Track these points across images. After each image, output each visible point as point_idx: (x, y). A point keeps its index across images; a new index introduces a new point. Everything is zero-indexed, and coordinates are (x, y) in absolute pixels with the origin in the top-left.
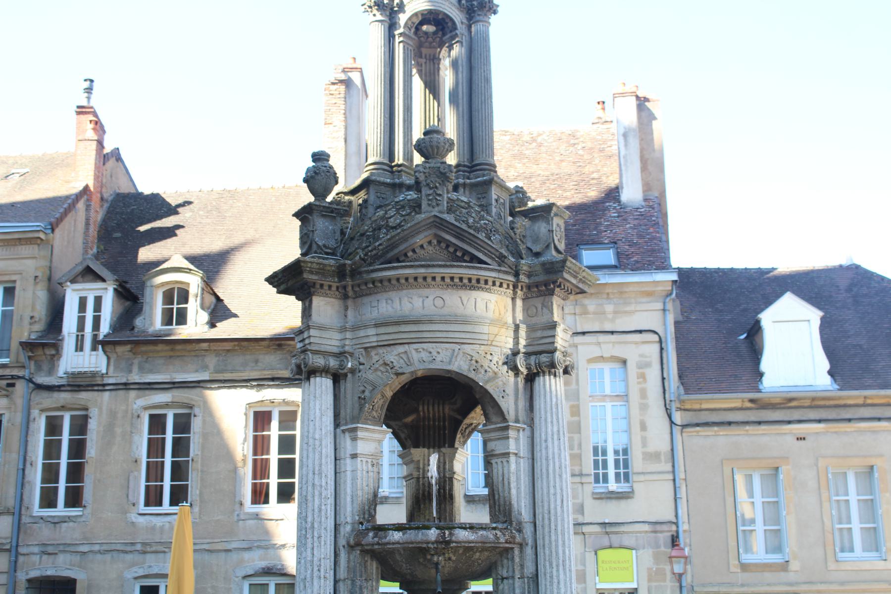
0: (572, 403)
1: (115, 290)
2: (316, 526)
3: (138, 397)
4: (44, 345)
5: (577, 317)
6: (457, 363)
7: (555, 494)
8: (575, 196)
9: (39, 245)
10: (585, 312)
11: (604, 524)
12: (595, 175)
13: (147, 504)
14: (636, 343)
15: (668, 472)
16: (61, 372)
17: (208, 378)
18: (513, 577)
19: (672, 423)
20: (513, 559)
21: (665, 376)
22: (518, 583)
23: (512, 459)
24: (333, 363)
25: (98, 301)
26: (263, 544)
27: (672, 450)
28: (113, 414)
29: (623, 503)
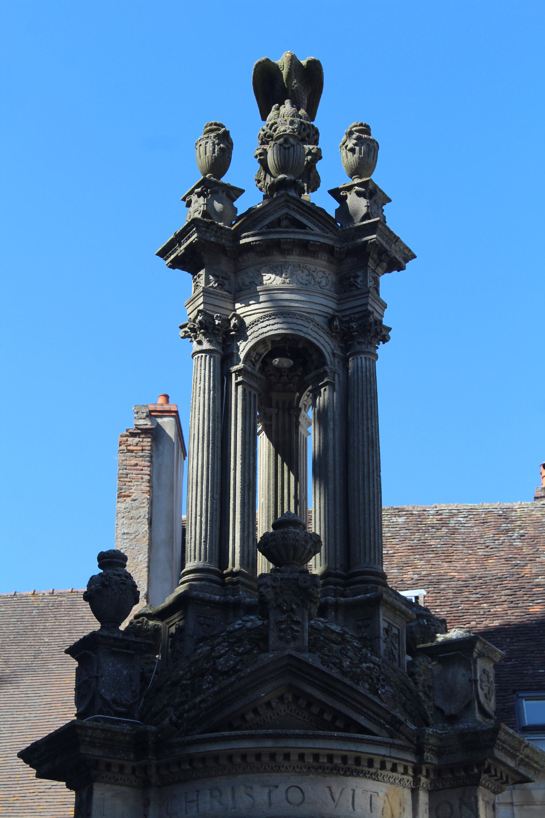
5: (516, 809)
8: (509, 612)
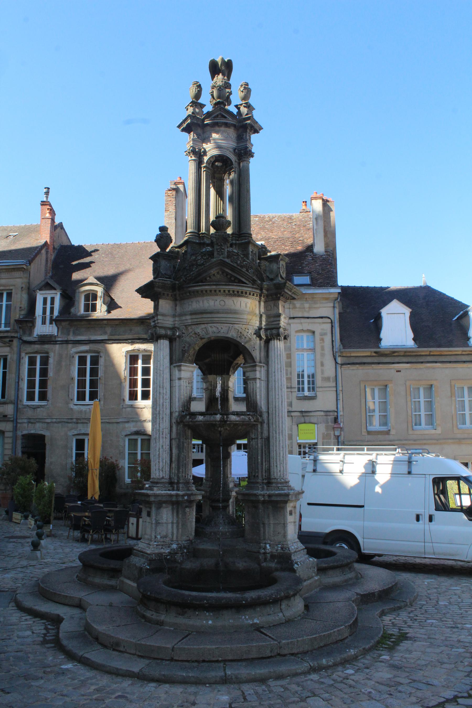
0: (287, 352)
1: (61, 294)
2: (161, 412)
3: (73, 347)
4: (26, 322)
6: (231, 334)
7: (278, 398)
9: (23, 271)
10: (295, 307)
11: (301, 412)
12: (301, 239)
13: (78, 400)
14: (320, 323)
15: (334, 387)
16: (35, 335)
17: (107, 338)
18: (257, 438)
19: (336, 363)
20: (257, 430)
21: (334, 339)
22: (259, 441)
23: (258, 381)
24: (169, 333)
25: (53, 299)
26: (135, 420)
27: (336, 376)
28: (60, 356)
29: (311, 402)
